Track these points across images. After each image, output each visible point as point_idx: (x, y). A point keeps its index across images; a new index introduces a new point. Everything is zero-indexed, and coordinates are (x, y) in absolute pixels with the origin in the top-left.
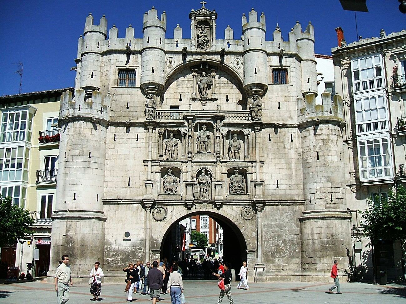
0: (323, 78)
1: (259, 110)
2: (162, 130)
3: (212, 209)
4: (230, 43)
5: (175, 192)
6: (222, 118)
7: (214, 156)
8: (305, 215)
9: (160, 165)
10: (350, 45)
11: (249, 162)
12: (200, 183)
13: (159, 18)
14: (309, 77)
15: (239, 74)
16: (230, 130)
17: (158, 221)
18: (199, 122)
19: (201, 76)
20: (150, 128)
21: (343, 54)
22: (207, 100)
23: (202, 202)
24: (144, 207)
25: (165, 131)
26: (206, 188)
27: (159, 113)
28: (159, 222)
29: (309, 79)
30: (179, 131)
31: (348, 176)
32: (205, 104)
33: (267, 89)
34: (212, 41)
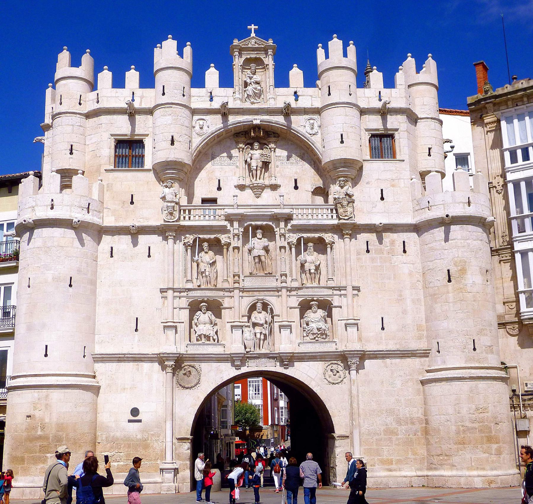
0: (452, 147)
2: (190, 238)
3: (275, 366)
4: (298, 94)
5: (214, 340)
6: (288, 218)
7: (277, 279)
8: (428, 374)
9: (187, 297)
10: (500, 91)
11: (334, 287)
12: (255, 325)
13: (181, 53)
14: (431, 147)
16: (303, 237)
17: (187, 388)
18: (251, 225)
20: (171, 236)
21: (487, 106)
22: (263, 188)
24: (164, 368)
25: (195, 241)
26: (264, 332)
27: (184, 211)
29: (430, 149)
30: (218, 241)
31: (501, 309)
32: (260, 195)
33: (361, 168)
34: (268, 90)
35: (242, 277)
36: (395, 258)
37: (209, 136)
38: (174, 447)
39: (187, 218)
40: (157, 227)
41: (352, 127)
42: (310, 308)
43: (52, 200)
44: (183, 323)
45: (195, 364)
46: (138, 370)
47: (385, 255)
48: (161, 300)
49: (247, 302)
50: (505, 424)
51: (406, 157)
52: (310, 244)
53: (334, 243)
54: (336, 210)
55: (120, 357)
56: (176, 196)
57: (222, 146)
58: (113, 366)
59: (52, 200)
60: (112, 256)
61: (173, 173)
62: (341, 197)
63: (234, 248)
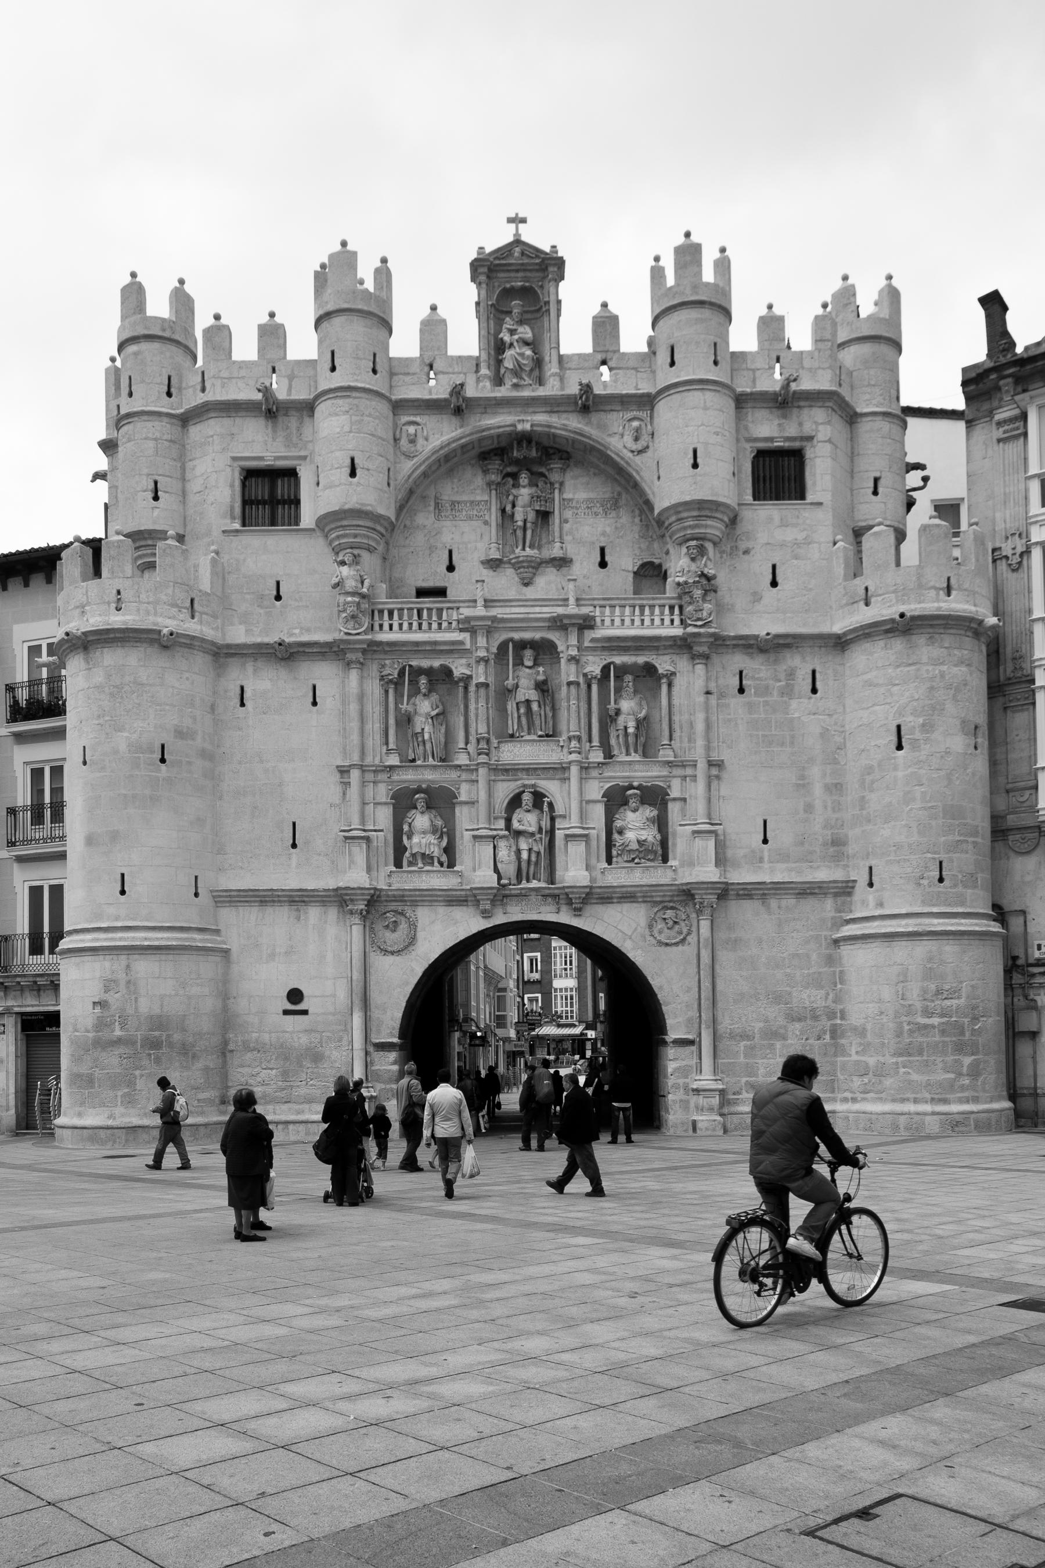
1: (706, 592)
5: (441, 864)
6: (586, 624)
12: (518, 833)
15: (642, 474)
17: (392, 953)
18: (512, 640)
19: (514, 486)
23: (523, 891)
25: (401, 673)
26: (535, 849)
28: (390, 959)
30: (447, 672)
32: (532, 579)
35: (494, 742)
36: (794, 704)
37: (427, 459)
38: (369, 1059)
39: (386, 627)
40: (328, 645)
41: (717, 434)
42: (625, 803)
43: (119, 592)
44: (382, 831)
45: (406, 908)
46: (298, 918)
47: (775, 697)
48: (339, 789)
49: (505, 790)
50: (991, 1020)
51: (826, 497)
52: (629, 678)
53: (673, 674)
54: (681, 607)
55: (264, 896)
56: (362, 583)
57: (456, 480)
58: (251, 914)
59: (119, 592)
60: (243, 704)
61: (355, 536)
62: (691, 581)
63: (478, 685)
